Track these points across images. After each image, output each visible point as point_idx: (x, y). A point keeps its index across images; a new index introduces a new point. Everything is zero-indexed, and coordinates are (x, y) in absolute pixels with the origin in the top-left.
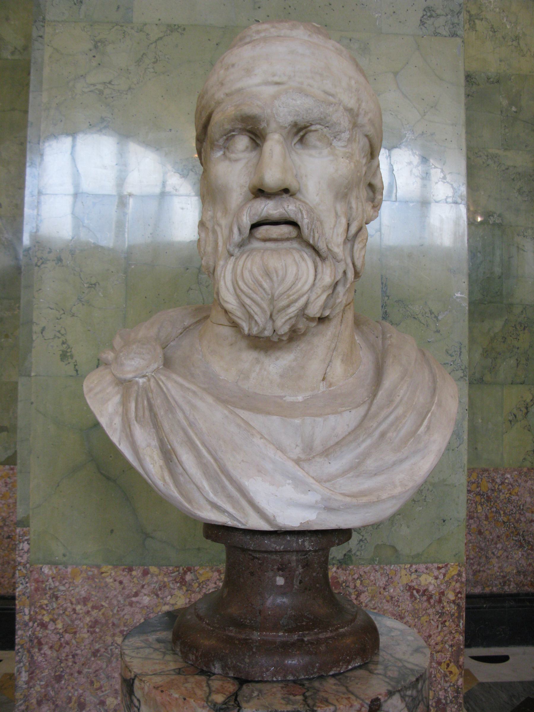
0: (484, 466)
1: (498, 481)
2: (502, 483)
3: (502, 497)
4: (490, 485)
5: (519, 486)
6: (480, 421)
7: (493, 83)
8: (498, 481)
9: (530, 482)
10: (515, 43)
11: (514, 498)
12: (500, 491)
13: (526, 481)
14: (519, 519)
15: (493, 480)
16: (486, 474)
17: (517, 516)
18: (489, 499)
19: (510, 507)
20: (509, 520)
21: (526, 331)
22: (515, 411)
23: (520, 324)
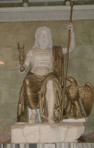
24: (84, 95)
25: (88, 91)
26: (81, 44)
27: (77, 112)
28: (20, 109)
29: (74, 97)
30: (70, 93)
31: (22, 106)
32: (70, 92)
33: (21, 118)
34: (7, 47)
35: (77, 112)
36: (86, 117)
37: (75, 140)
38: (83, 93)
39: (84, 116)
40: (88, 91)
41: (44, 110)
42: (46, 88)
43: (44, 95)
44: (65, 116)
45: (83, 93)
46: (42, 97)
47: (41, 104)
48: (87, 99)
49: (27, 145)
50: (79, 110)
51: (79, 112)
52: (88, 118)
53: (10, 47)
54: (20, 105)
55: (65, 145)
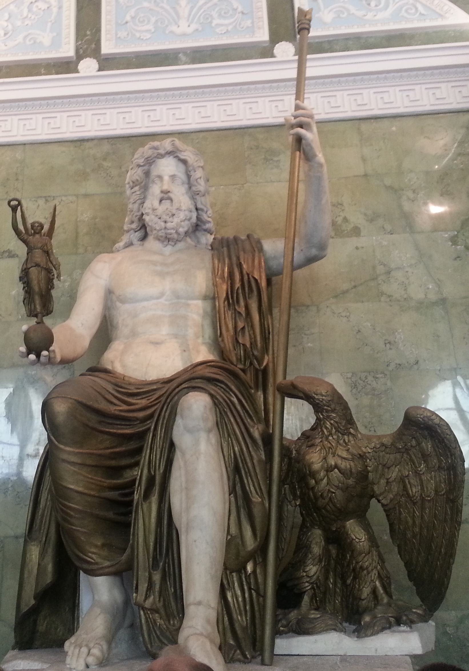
24: (402, 480)
25: (425, 457)
27: (366, 592)
28: (35, 571)
29: (339, 496)
30: (313, 474)
31: (42, 554)
32: (316, 466)
35: (366, 592)
36: (424, 619)
38: (394, 474)
39: (414, 617)
40: (425, 457)
41: (157, 577)
42: (172, 446)
43: (160, 485)
44: (293, 615)
45: (394, 474)
46: (147, 496)
47: (141, 540)
48: (423, 508)
50: (374, 574)
51: (374, 591)
52: (432, 623)
54: (34, 552)
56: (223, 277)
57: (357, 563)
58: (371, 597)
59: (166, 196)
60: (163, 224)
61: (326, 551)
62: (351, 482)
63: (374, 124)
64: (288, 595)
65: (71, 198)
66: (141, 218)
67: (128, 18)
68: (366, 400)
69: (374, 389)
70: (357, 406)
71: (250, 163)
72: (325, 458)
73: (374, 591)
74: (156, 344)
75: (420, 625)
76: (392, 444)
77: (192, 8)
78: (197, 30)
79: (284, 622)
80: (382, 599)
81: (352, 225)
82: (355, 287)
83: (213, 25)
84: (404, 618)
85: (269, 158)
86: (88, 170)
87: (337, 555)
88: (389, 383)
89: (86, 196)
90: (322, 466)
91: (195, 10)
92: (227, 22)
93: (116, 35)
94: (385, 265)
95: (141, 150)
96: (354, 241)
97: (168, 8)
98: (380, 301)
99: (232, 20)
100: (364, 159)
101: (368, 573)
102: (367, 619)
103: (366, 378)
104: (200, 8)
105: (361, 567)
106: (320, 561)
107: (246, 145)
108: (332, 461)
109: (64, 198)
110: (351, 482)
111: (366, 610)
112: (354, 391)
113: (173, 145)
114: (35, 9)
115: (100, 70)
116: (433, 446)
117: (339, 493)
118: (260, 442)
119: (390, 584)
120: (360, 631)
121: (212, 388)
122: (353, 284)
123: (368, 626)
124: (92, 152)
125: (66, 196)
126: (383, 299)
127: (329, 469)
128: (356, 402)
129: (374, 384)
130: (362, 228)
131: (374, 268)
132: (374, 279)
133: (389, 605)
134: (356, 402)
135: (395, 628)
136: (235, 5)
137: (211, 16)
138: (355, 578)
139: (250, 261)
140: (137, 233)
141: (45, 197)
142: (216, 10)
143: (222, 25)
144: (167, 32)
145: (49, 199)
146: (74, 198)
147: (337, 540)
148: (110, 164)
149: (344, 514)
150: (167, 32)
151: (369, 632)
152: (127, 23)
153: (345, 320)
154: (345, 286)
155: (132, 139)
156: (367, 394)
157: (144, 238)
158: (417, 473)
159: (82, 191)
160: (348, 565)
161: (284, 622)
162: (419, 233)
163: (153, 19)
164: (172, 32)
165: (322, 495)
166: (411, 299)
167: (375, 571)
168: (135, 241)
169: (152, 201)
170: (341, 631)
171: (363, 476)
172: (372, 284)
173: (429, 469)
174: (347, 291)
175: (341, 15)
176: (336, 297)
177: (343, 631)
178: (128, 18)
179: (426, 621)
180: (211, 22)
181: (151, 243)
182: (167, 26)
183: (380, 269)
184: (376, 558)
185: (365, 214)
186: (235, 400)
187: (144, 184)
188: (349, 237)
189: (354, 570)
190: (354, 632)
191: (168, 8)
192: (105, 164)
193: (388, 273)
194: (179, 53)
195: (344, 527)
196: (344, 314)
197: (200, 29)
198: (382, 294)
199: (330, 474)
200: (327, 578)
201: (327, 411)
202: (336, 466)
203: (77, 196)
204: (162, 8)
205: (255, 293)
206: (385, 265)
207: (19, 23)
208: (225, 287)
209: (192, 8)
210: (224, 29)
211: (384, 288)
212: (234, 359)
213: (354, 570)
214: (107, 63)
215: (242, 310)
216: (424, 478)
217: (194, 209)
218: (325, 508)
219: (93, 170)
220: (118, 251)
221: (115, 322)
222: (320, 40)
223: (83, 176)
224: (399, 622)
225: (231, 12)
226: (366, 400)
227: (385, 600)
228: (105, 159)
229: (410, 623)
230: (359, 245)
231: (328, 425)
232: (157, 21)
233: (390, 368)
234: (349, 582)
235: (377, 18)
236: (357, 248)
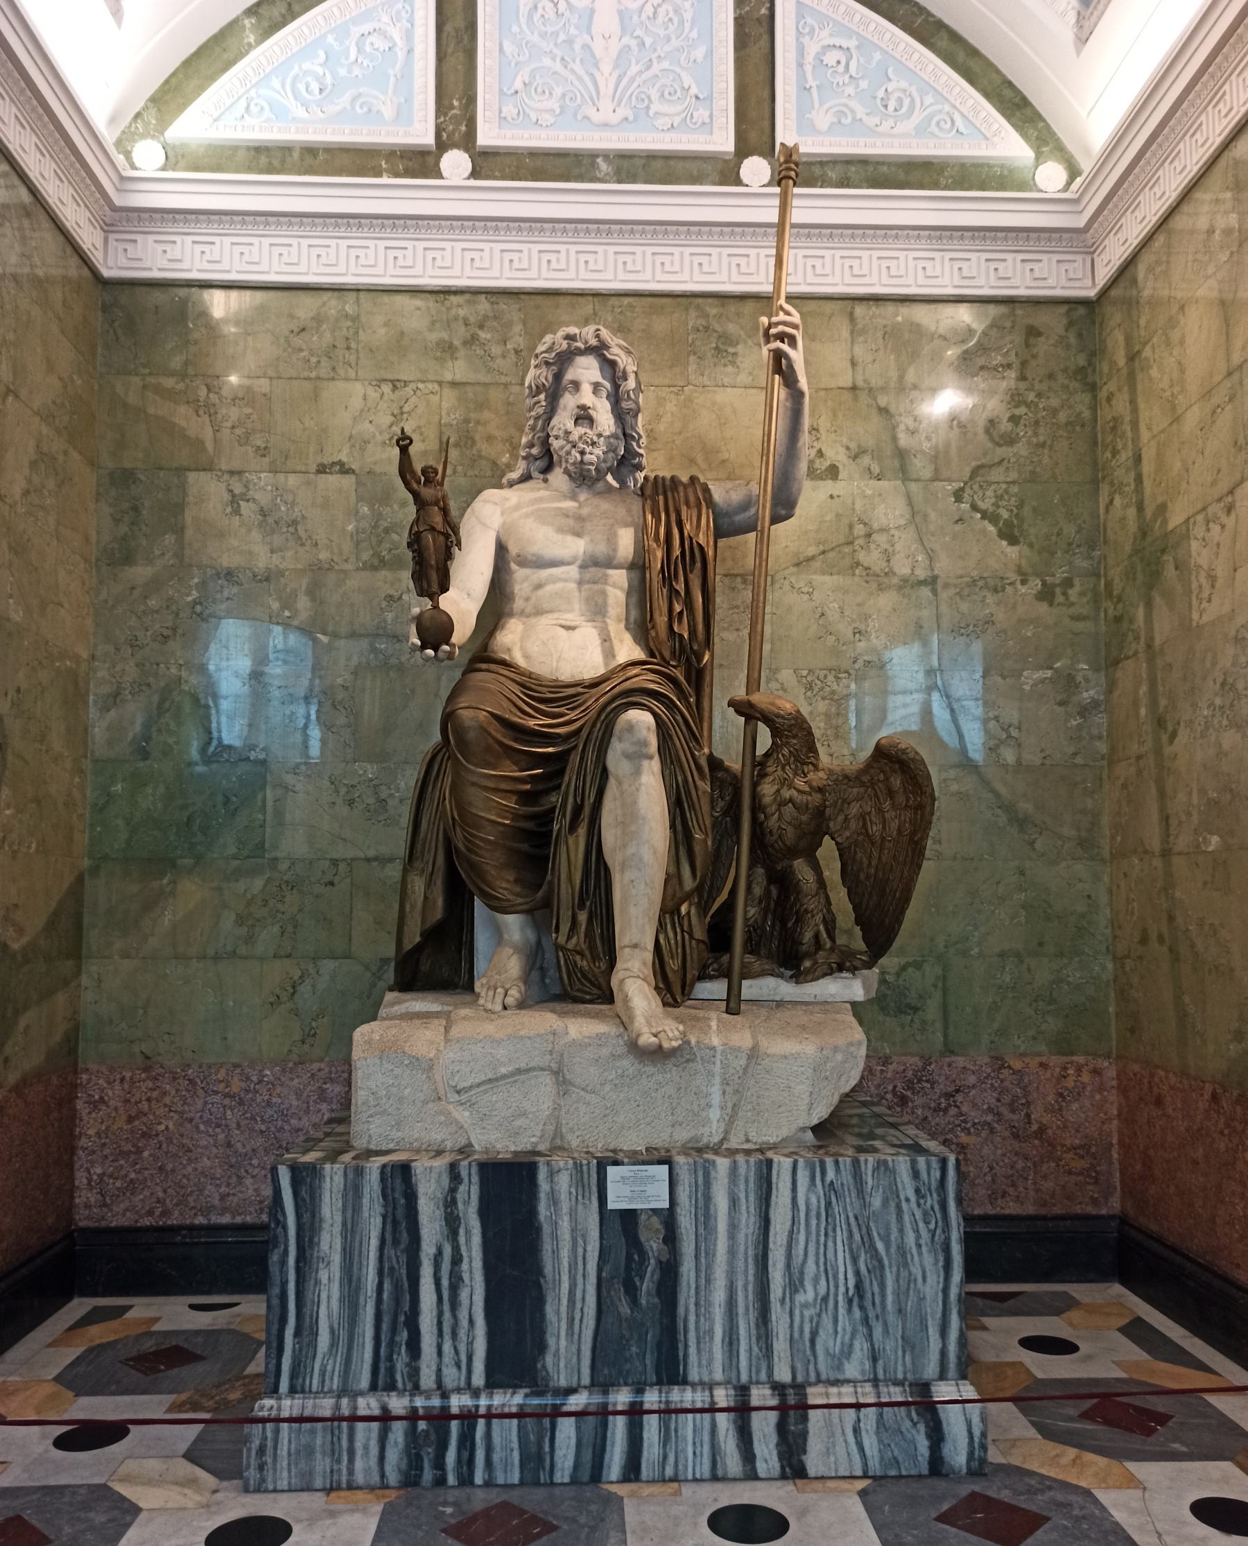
0: (235, 1060)
1: (254, 1078)
2: (260, 1082)
3: (259, 1099)
4: (243, 1085)
5: (282, 1085)
6: (231, 1003)
7: (261, 581)
8: (254, 1078)
9: (296, 1081)
10: (291, 529)
11: (274, 1100)
12: (257, 1092)
13: (292, 1079)
14: (282, 1128)
15: (248, 1078)
16: (238, 1071)
17: (280, 1123)
18: (241, 1102)
19: (270, 1112)
20: (268, 1128)
21: (295, 891)
22: (278, 991)
23: (287, 882)
25: (891, 793)
26: (833, 472)
29: (790, 834)
33: (425, 966)
34: (322, 469)
35: (808, 936)
37: (803, 1129)
38: (854, 809)
49: (464, 1174)
51: (817, 936)
53: (344, 470)
55: (734, 1168)
56: (657, 539)
57: (802, 905)
58: (813, 941)
59: (584, 416)
60: (578, 456)
61: (767, 892)
62: (804, 818)
63: (874, 309)
64: (719, 937)
65: (430, 386)
66: (545, 443)
67: (518, 85)
68: (822, 706)
69: (833, 692)
70: (811, 713)
71: (695, 353)
72: (778, 791)
73: (817, 936)
74: (569, 628)
75: (865, 972)
76: (856, 777)
77: (620, 78)
78: (626, 119)
79: (715, 966)
80: (825, 944)
81: (829, 463)
82: (824, 552)
83: (651, 113)
84: (848, 964)
85: (721, 346)
86: (456, 343)
87: (779, 896)
88: (853, 686)
89: (454, 384)
90: (775, 800)
91: (625, 81)
92: (671, 109)
93: (500, 112)
94: (865, 524)
95: (548, 338)
96: (828, 487)
97: (582, 73)
98: (854, 575)
99: (680, 108)
100: (853, 364)
101: (813, 916)
102: (807, 964)
103: (825, 677)
104: (632, 80)
105: (806, 911)
106: (760, 902)
107: (691, 324)
108: (786, 793)
109: (421, 386)
110: (804, 818)
111: (807, 955)
112: (809, 693)
113: (598, 336)
114: (368, 49)
115: (475, 174)
116: (902, 782)
117: (790, 830)
118: (706, 770)
119: (834, 928)
120: (799, 977)
121: (654, 704)
122: (821, 548)
123: (808, 971)
124: (461, 312)
125: (423, 382)
126: (857, 572)
127: (782, 803)
128: (810, 708)
129: (835, 687)
130: (841, 467)
131: (851, 527)
132: (851, 543)
133: (832, 950)
134: (810, 708)
135: (836, 974)
136: (687, 80)
137: (649, 97)
138: (797, 921)
139: (695, 520)
140: (538, 463)
141: (391, 381)
142: (656, 87)
143: (666, 115)
144: (579, 117)
145: (398, 384)
146: (436, 386)
147: (783, 882)
148: (489, 336)
149: (793, 853)
150: (579, 117)
151: (809, 978)
152: (516, 92)
153: (806, 597)
154: (812, 551)
155: (523, 297)
156: (823, 699)
157: (548, 469)
158: (880, 811)
159: (448, 377)
160: (791, 908)
161: (715, 966)
162: (915, 480)
163: (558, 91)
164: (586, 118)
165: (771, 832)
166: (894, 574)
167: (820, 915)
168: (535, 474)
169: (563, 420)
170: (778, 976)
171: (820, 813)
172: (847, 550)
173: (894, 807)
174: (813, 558)
175: (843, 120)
176: (797, 565)
177: (781, 976)
178: (518, 85)
179: (870, 968)
180: (648, 108)
181: (558, 477)
182: (580, 106)
183: (859, 530)
184: (823, 900)
185: (848, 448)
186: (679, 718)
187: (554, 392)
188: (822, 479)
189: (797, 912)
190: (791, 977)
191: (582, 73)
192: (483, 335)
193: (869, 535)
194: (598, 156)
195: (791, 866)
196: (805, 590)
197: (631, 118)
198: (858, 564)
199: (782, 809)
200: (764, 920)
201: (787, 737)
202: (791, 800)
203: (440, 383)
204: (572, 71)
205: (698, 565)
206: (865, 524)
207: (342, 72)
208: (659, 554)
209: (620, 78)
210: (667, 122)
211: (862, 556)
212: (667, 654)
213: (797, 912)
214: (489, 164)
215: (680, 587)
216: (887, 815)
217: (621, 436)
218: (772, 846)
219: (465, 343)
220: (511, 486)
221: (508, 590)
222: (810, 159)
223: (447, 350)
224: (841, 968)
225: (679, 94)
226: (822, 706)
227: (828, 945)
228: (481, 327)
229: (853, 970)
230: (835, 494)
231: (786, 751)
232: (564, 95)
233: (857, 666)
234: (790, 925)
235: (895, 131)
236: (832, 497)
